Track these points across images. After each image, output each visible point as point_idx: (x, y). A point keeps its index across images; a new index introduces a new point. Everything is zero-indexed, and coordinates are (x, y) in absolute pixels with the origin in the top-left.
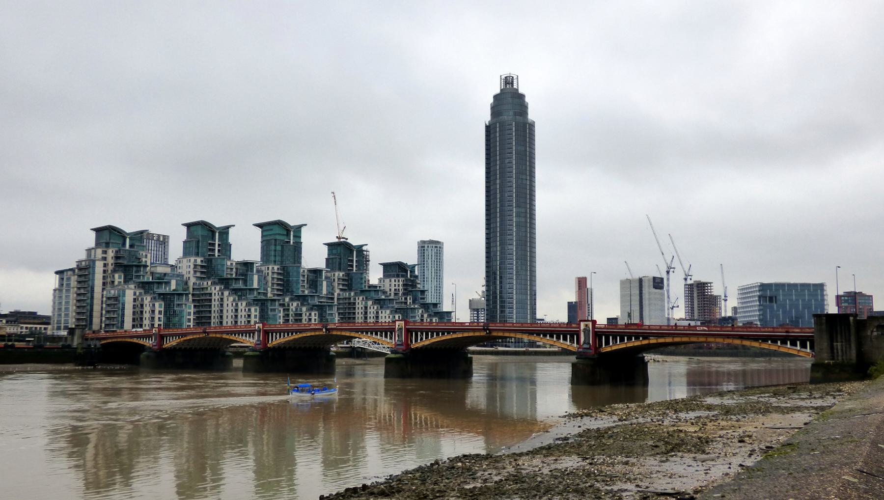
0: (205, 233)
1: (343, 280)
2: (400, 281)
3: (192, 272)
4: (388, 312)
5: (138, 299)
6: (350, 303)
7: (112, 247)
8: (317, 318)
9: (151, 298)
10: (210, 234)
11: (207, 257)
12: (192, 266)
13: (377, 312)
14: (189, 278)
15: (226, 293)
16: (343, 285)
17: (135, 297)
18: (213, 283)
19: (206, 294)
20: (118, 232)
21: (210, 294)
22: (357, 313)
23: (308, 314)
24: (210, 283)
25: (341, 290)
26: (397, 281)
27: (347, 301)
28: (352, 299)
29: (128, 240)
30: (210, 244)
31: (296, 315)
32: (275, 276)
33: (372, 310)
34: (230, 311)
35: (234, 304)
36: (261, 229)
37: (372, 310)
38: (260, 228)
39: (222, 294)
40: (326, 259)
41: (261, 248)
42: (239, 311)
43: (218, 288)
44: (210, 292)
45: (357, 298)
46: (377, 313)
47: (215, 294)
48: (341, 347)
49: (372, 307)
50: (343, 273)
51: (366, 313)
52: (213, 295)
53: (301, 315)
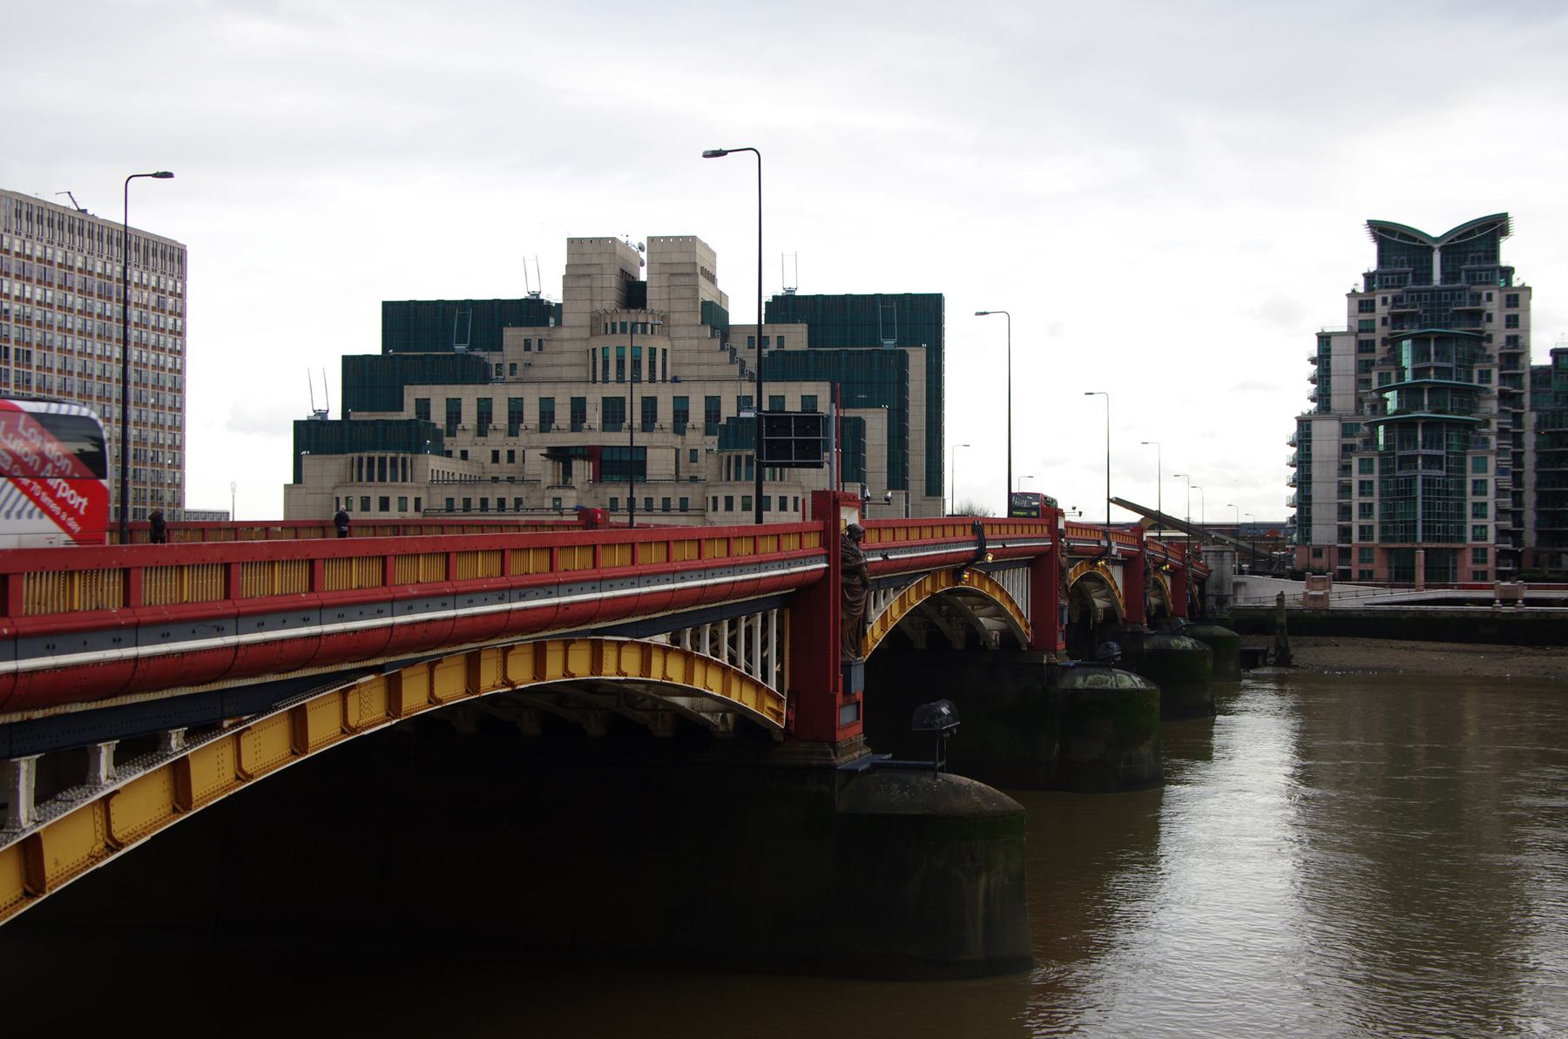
7: (1380, 287)
20: (1402, 236)
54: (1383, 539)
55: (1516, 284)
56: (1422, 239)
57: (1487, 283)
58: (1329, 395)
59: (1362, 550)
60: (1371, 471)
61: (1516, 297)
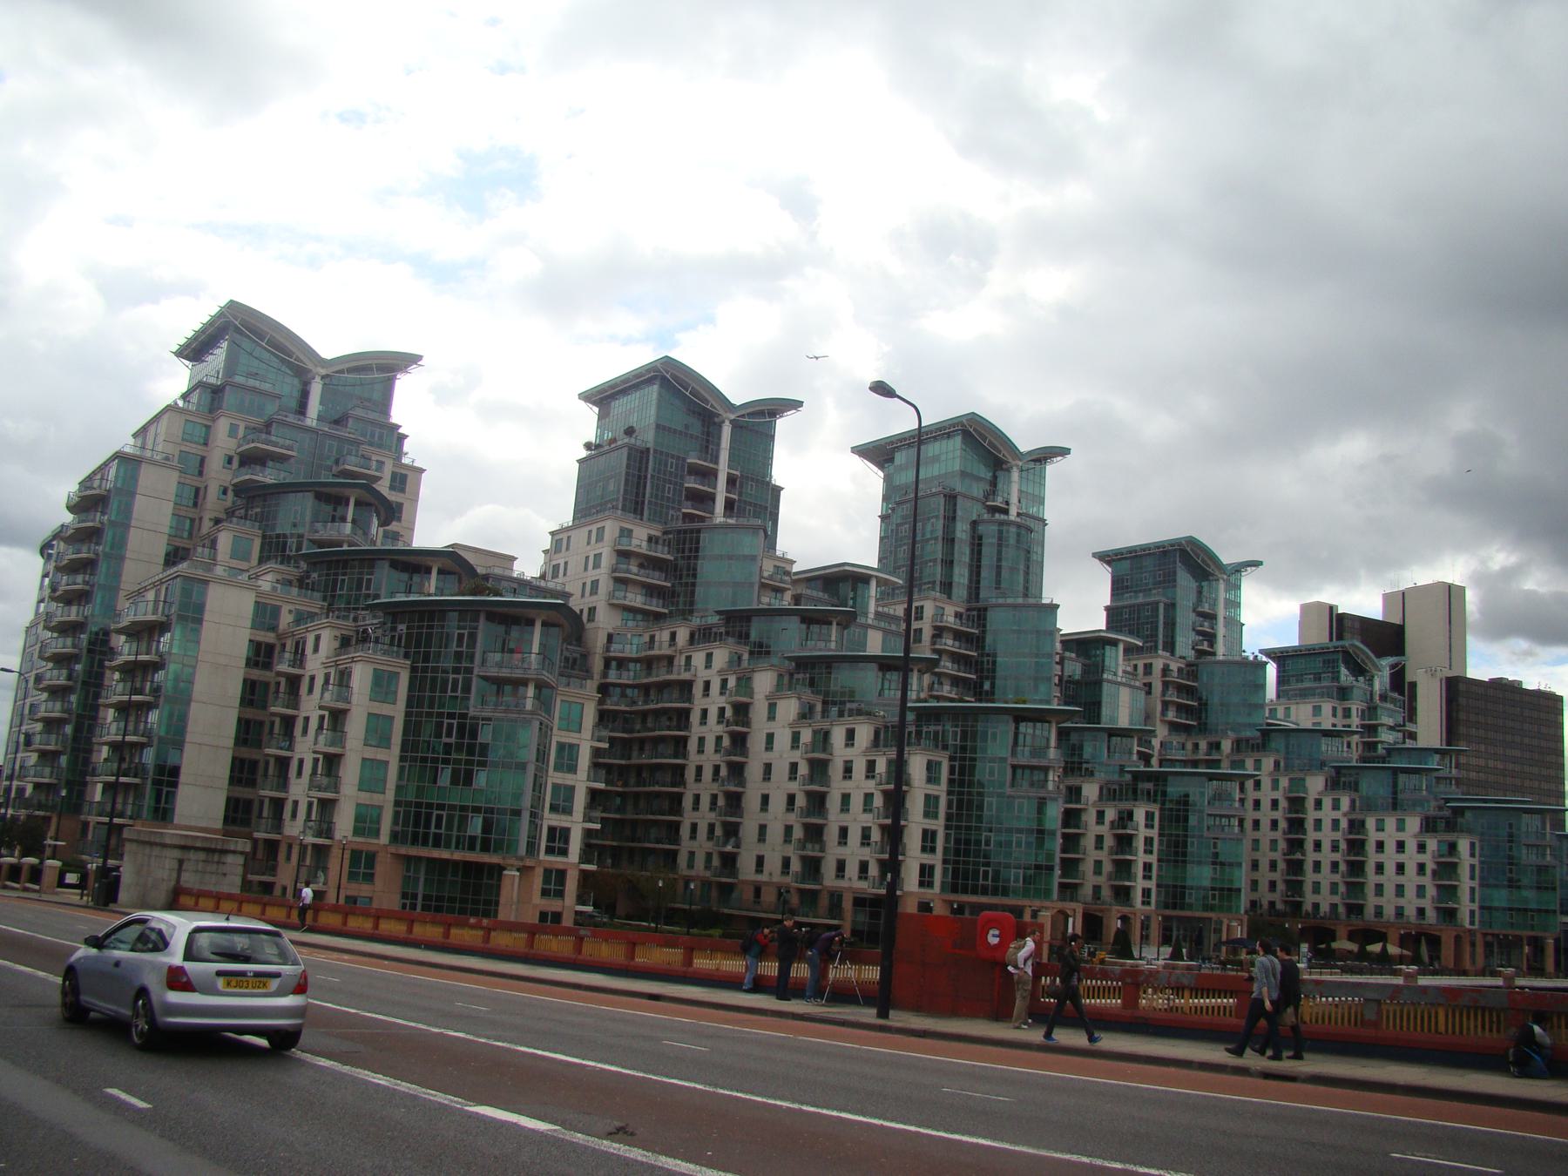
0: (679, 419)
1: (1180, 688)
2: (1354, 712)
3: (605, 586)
4: (1413, 824)
5: (284, 645)
8: (1154, 833)
9: (345, 642)
10: (697, 428)
11: (680, 525)
12: (607, 560)
13: (1351, 823)
14: (592, 610)
15: (764, 682)
16: (1180, 708)
17: (269, 637)
18: (702, 636)
19: (663, 686)
21: (686, 687)
23: (1111, 814)
24: (683, 635)
25: (1174, 727)
26: (1340, 712)
29: (316, 390)
30: (697, 471)
32: (948, 643)
33: (1327, 814)
34: (781, 771)
35: (806, 736)
37: (1327, 814)
38: (881, 466)
39: (745, 682)
40: (1107, 609)
41: (881, 539)
42: (836, 770)
43: (721, 656)
44: (685, 676)
46: (1356, 826)
47: (707, 685)
49: (1327, 803)
51: (1297, 825)
52: (698, 690)
54: (395, 837)
55: (405, 461)
56: (302, 357)
57: (380, 446)
58: (122, 558)
59: (356, 856)
61: (404, 478)
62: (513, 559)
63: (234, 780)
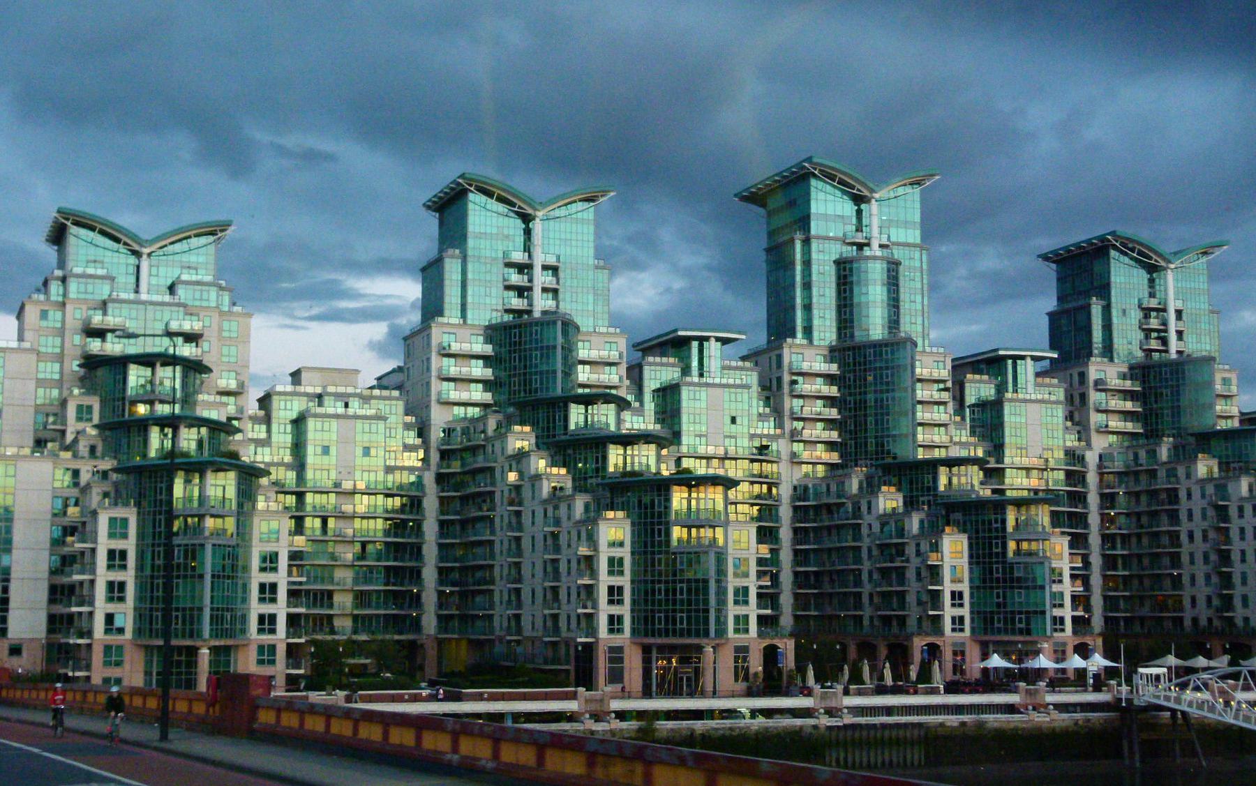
6: (1153, 494)
22: (1184, 538)
27: (1143, 485)
28: (1162, 473)
31: (882, 547)
36: (761, 211)
40: (1050, 315)
45: (1181, 471)
48: (1062, 707)
50: (1124, 369)
53: (900, 550)
59: (108, 649)
60: (125, 536)
62: (357, 371)
63: (52, 600)
